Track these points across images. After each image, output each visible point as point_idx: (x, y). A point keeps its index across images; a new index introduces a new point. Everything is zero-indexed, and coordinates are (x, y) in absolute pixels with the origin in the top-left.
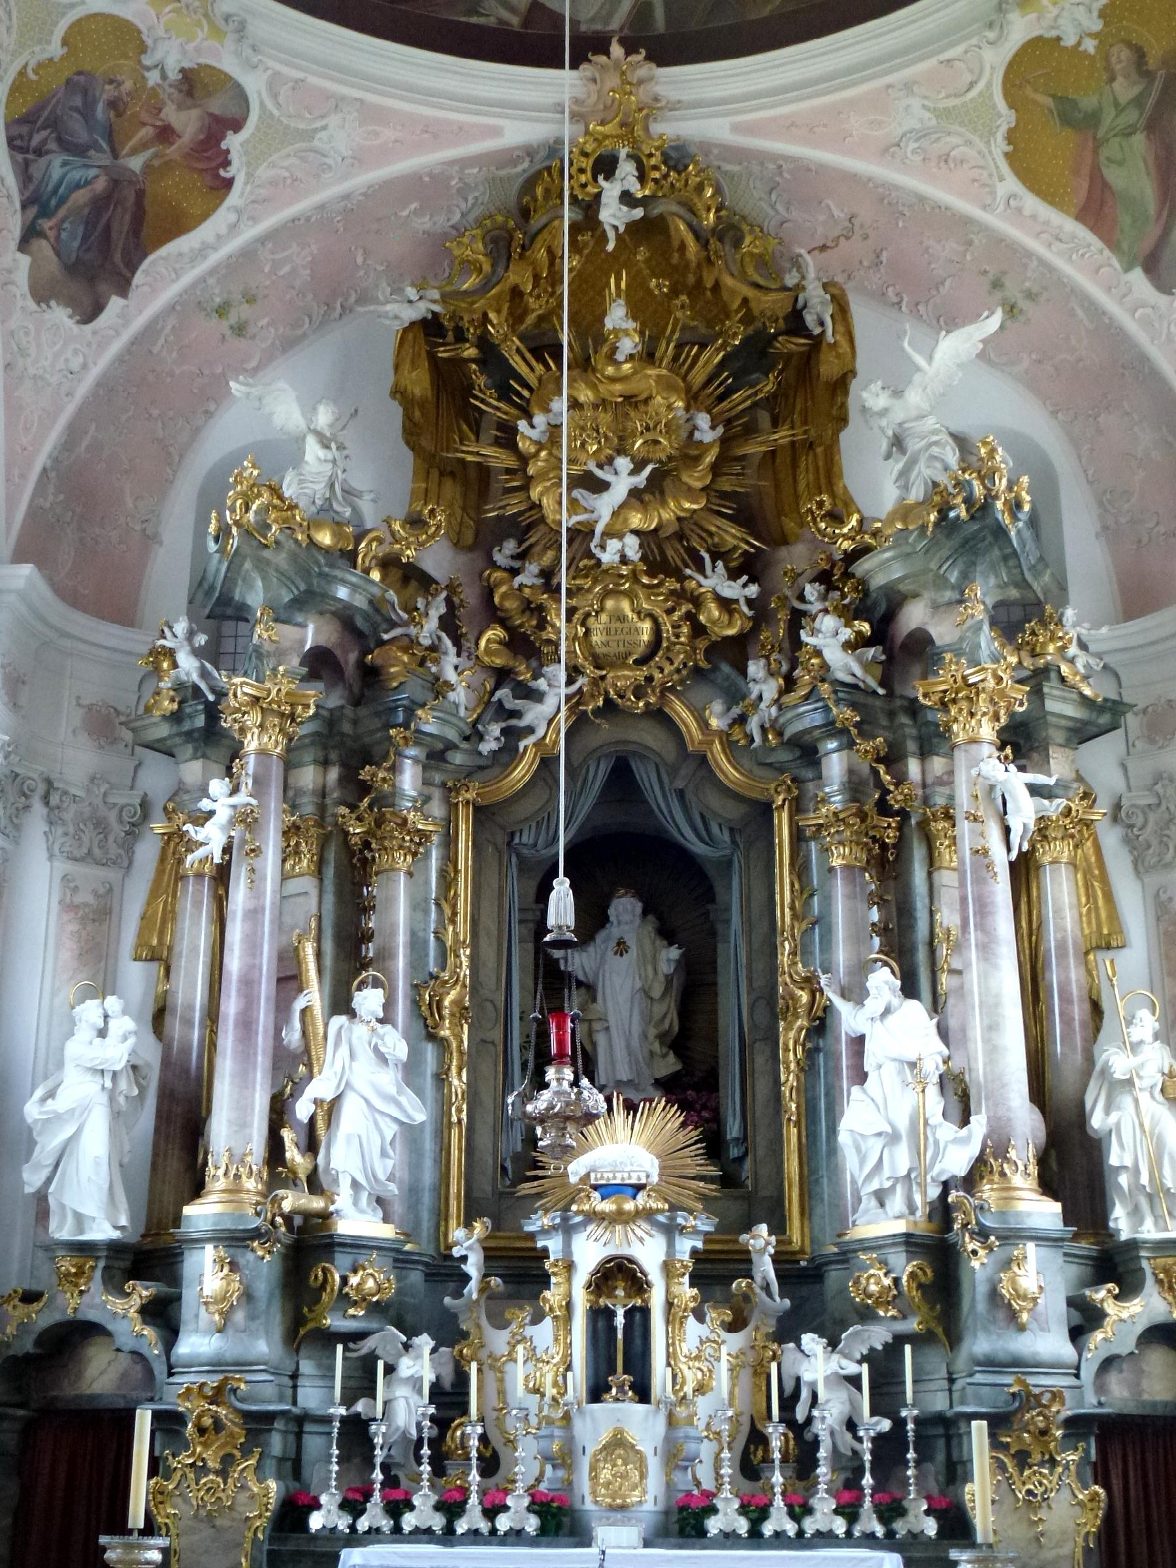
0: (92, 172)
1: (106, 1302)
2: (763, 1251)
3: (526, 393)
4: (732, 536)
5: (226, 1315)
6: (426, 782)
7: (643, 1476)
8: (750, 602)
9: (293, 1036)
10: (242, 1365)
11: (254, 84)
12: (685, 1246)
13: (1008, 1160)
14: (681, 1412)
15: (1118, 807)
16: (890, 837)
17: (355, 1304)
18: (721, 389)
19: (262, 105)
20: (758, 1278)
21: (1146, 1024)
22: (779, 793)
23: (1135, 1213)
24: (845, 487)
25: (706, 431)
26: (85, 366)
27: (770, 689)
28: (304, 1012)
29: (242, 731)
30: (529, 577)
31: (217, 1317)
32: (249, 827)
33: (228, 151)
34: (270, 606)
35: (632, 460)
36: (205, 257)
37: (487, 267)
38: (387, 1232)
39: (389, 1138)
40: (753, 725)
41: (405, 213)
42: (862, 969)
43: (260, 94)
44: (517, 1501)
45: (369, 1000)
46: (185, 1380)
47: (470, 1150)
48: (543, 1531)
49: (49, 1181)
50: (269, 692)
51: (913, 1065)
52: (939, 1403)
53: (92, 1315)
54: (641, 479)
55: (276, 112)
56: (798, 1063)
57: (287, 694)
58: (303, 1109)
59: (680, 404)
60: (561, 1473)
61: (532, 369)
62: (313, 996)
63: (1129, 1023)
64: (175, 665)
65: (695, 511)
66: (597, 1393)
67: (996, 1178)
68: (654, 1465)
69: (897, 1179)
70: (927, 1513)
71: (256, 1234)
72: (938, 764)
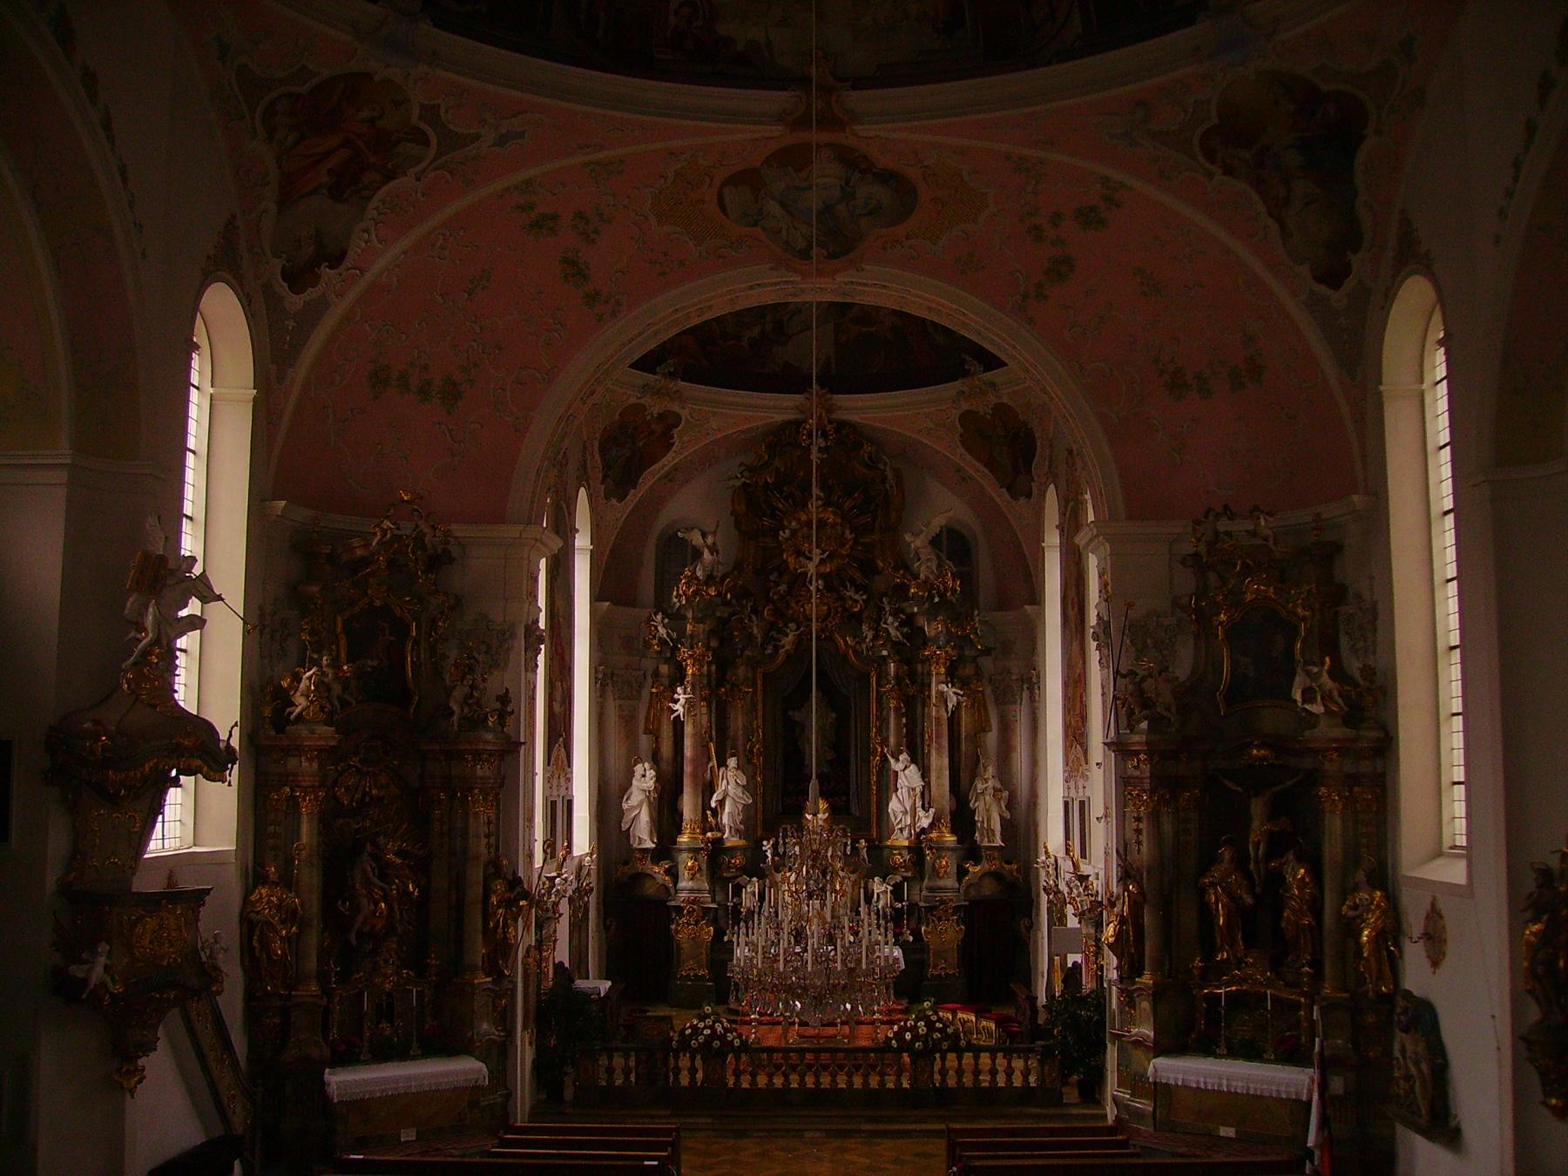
4: (858, 576)
5: (693, 875)
8: (863, 600)
10: (699, 891)
11: (684, 413)
19: (687, 419)
21: (991, 771)
26: (622, 516)
27: (870, 635)
30: (783, 588)
34: (693, 618)
38: (742, 842)
45: (732, 762)
49: (630, 827)
50: (696, 653)
51: (914, 789)
53: (649, 871)
55: (691, 420)
58: (713, 805)
59: (840, 521)
63: (985, 771)
70: (910, 934)
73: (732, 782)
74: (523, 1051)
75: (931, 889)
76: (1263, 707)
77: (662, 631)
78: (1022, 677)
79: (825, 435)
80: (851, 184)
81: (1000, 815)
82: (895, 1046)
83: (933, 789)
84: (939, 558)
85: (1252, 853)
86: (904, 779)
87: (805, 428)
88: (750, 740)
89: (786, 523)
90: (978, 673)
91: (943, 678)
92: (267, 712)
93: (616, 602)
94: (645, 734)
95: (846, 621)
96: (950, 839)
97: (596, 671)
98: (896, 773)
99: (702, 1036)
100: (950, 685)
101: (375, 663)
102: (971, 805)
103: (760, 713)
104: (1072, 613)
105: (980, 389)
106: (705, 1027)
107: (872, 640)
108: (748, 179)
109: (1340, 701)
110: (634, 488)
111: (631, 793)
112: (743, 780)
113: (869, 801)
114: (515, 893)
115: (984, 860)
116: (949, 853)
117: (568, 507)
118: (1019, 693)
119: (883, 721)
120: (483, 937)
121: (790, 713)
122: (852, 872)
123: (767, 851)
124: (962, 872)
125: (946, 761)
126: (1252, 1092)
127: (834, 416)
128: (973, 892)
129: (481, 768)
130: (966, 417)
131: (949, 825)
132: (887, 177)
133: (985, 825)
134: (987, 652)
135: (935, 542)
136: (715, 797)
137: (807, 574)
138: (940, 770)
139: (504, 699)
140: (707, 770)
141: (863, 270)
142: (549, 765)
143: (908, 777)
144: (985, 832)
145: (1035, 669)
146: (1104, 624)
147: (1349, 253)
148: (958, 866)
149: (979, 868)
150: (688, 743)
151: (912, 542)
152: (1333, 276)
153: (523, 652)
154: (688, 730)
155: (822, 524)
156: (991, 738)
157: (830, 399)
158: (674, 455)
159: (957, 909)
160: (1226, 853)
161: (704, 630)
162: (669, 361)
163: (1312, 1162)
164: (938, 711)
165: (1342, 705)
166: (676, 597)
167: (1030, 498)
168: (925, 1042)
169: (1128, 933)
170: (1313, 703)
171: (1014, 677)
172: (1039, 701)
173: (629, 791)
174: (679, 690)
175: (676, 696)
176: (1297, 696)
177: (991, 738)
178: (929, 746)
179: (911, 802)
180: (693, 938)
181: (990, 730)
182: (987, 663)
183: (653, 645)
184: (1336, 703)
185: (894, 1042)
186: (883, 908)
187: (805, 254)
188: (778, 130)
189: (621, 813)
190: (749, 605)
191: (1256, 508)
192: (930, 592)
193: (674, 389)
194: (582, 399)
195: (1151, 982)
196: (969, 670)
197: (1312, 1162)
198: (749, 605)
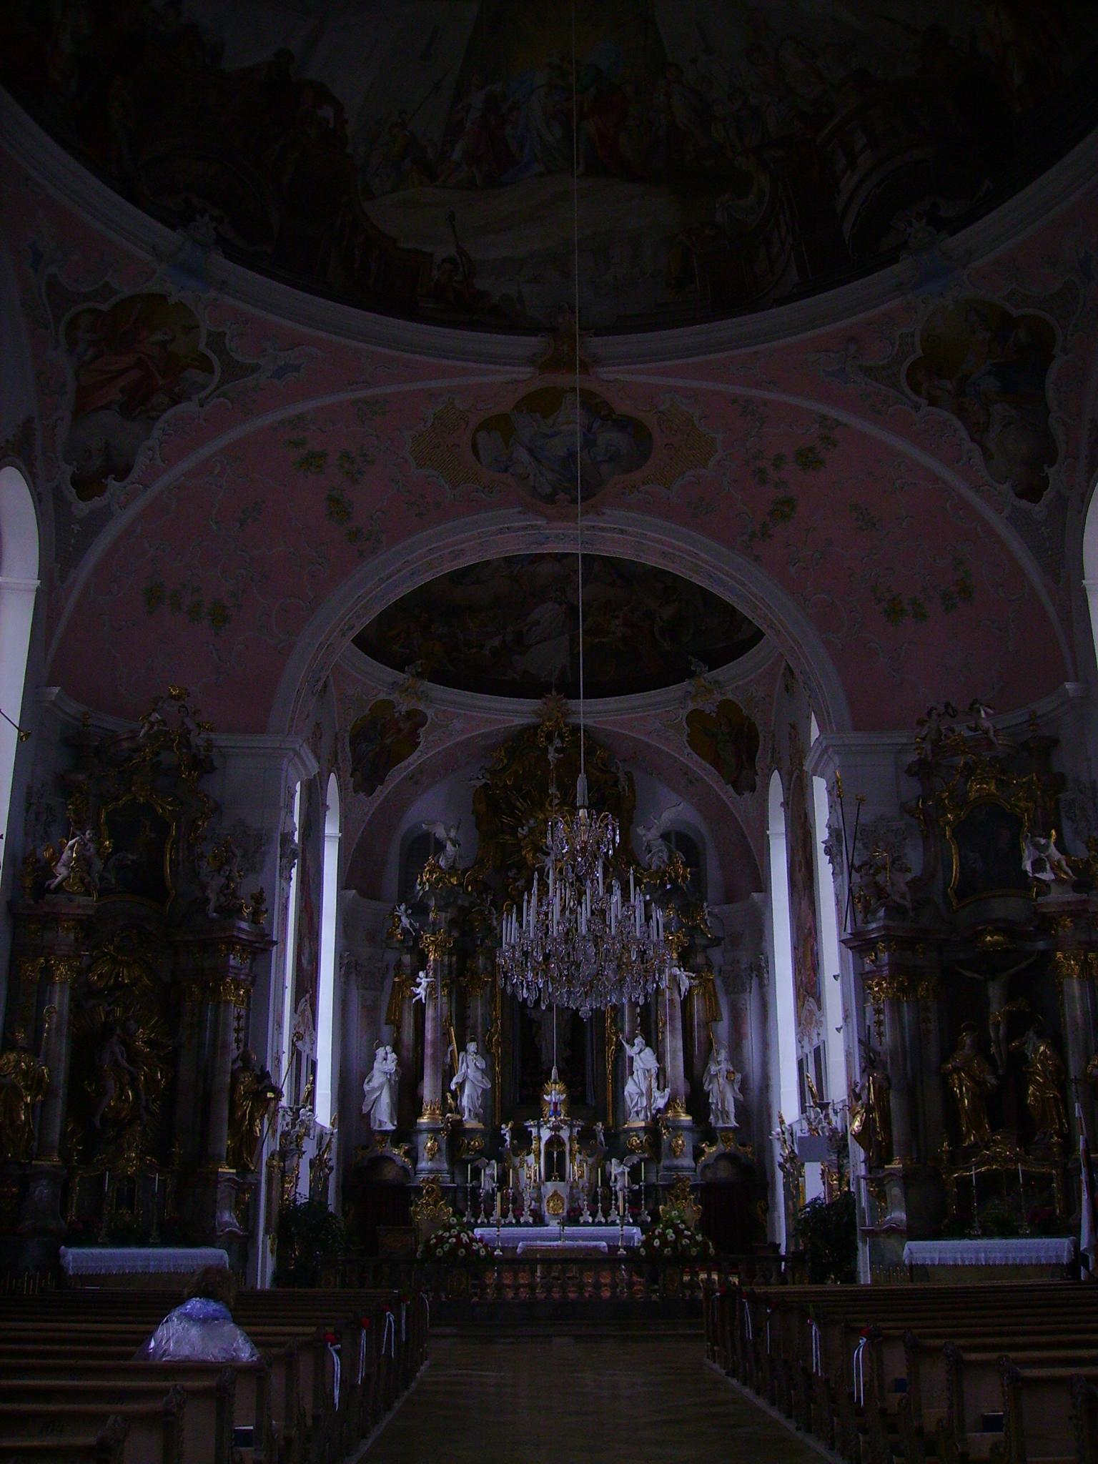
0: (374, 747)
5: (433, 1156)
7: (563, 1204)
10: (439, 1171)
11: (429, 713)
13: (676, 1102)
14: (575, 1185)
15: (721, 969)
17: (472, 1150)
19: (432, 719)
21: (723, 1055)
23: (716, 1117)
26: (368, 812)
28: (451, 1051)
29: (429, 951)
37: (505, 761)
38: (480, 1126)
39: (480, 1092)
43: (431, 715)
44: (526, 1212)
45: (472, 1047)
46: (422, 1176)
48: (534, 1221)
50: (438, 939)
56: (612, 1062)
58: (453, 1087)
60: (538, 1204)
61: (522, 805)
63: (718, 1054)
64: (401, 921)
66: (548, 1179)
67: (673, 1108)
68: (566, 1200)
69: (642, 1108)
71: (442, 1129)
73: (472, 1065)
74: (264, 1257)
75: (668, 1168)
76: (994, 897)
77: (405, 921)
78: (751, 966)
79: (561, 736)
80: (593, 430)
81: (734, 1098)
82: (644, 1254)
83: (669, 1070)
84: (670, 850)
85: (992, 1035)
86: (638, 1059)
87: (542, 731)
88: (490, 1031)
89: (524, 822)
90: (709, 964)
91: (675, 962)
92: (28, 882)
93: (362, 893)
94: (386, 1024)
96: (685, 1118)
98: (631, 1059)
99: (447, 1245)
100: (682, 969)
101: (135, 858)
102: (705, 1088)
103: (499, 1004)
104: (799, 877)
105: (704, 687)
106: (449, 1237)
108: (500, 424)
109: (1070, 872)
111: (372, 1077)
112: (482, 1064)
113: (605, 1089)
114: (263, 1085)
115: (719, 1140)
116: (685, 1133)
120: (229, 1129)
123: (505, 1134)
124: (698, 1153)
125: (680, 1044)
126: (1010, 1262)
128: (709, 1174)
129: (234, 958)
130: (694, 717)
131: (684, 1105)
132: (627, 424)
133: (720, 1107)
134: (716, 941)
135: (665, 836)
136: (455, 1080)
137: (544, 869)
138: (674, 1052)
139: (259, 898)
140: (446, 1054)
141: (603, 514)
142: (296, 1012)
143: (643, 1059)
145: (762, 954)
146: (835, 833)
147: (1045, 467)
148: (693, 1147)
149: (714, 1149)
150: (429, 1026)
151: (644, 835)
152: (1031, 491)
153: (279, 859)
154: (430, 1013)
156: (723, 1028)
158: (420, 753)
159: (694, 1188)
160: (967, 1039)
161: (446, 918)
162: (417, 662)
163: (1087, 1268)
164: (672, 993)
165: (1071, 874)
166: (420, 885)
167: (754, 792)
168: (674, 1248)
169: (874, 1119)
170: (1043, 872)
171: (743, 967)
172: (768, 985)
174: (421, 974)
175: (418, 980)
176: (1028, 866)
177: (723, 1028)
178: (663, 1033)
179: (648, 1082)
180: (431, 1219)
182: (716, 955)
183: (396, 935)
184: (1066, 873)
185: (642, 1249)
187: (550, 499)
188: (525, 372)
189: (363, 1095)
191: (976, 701)
192: (662, 880)
193: (421, 689)
194: (341, 630)
195: (901, 1166)
196: (700, 960)
197: (1087, 1268)
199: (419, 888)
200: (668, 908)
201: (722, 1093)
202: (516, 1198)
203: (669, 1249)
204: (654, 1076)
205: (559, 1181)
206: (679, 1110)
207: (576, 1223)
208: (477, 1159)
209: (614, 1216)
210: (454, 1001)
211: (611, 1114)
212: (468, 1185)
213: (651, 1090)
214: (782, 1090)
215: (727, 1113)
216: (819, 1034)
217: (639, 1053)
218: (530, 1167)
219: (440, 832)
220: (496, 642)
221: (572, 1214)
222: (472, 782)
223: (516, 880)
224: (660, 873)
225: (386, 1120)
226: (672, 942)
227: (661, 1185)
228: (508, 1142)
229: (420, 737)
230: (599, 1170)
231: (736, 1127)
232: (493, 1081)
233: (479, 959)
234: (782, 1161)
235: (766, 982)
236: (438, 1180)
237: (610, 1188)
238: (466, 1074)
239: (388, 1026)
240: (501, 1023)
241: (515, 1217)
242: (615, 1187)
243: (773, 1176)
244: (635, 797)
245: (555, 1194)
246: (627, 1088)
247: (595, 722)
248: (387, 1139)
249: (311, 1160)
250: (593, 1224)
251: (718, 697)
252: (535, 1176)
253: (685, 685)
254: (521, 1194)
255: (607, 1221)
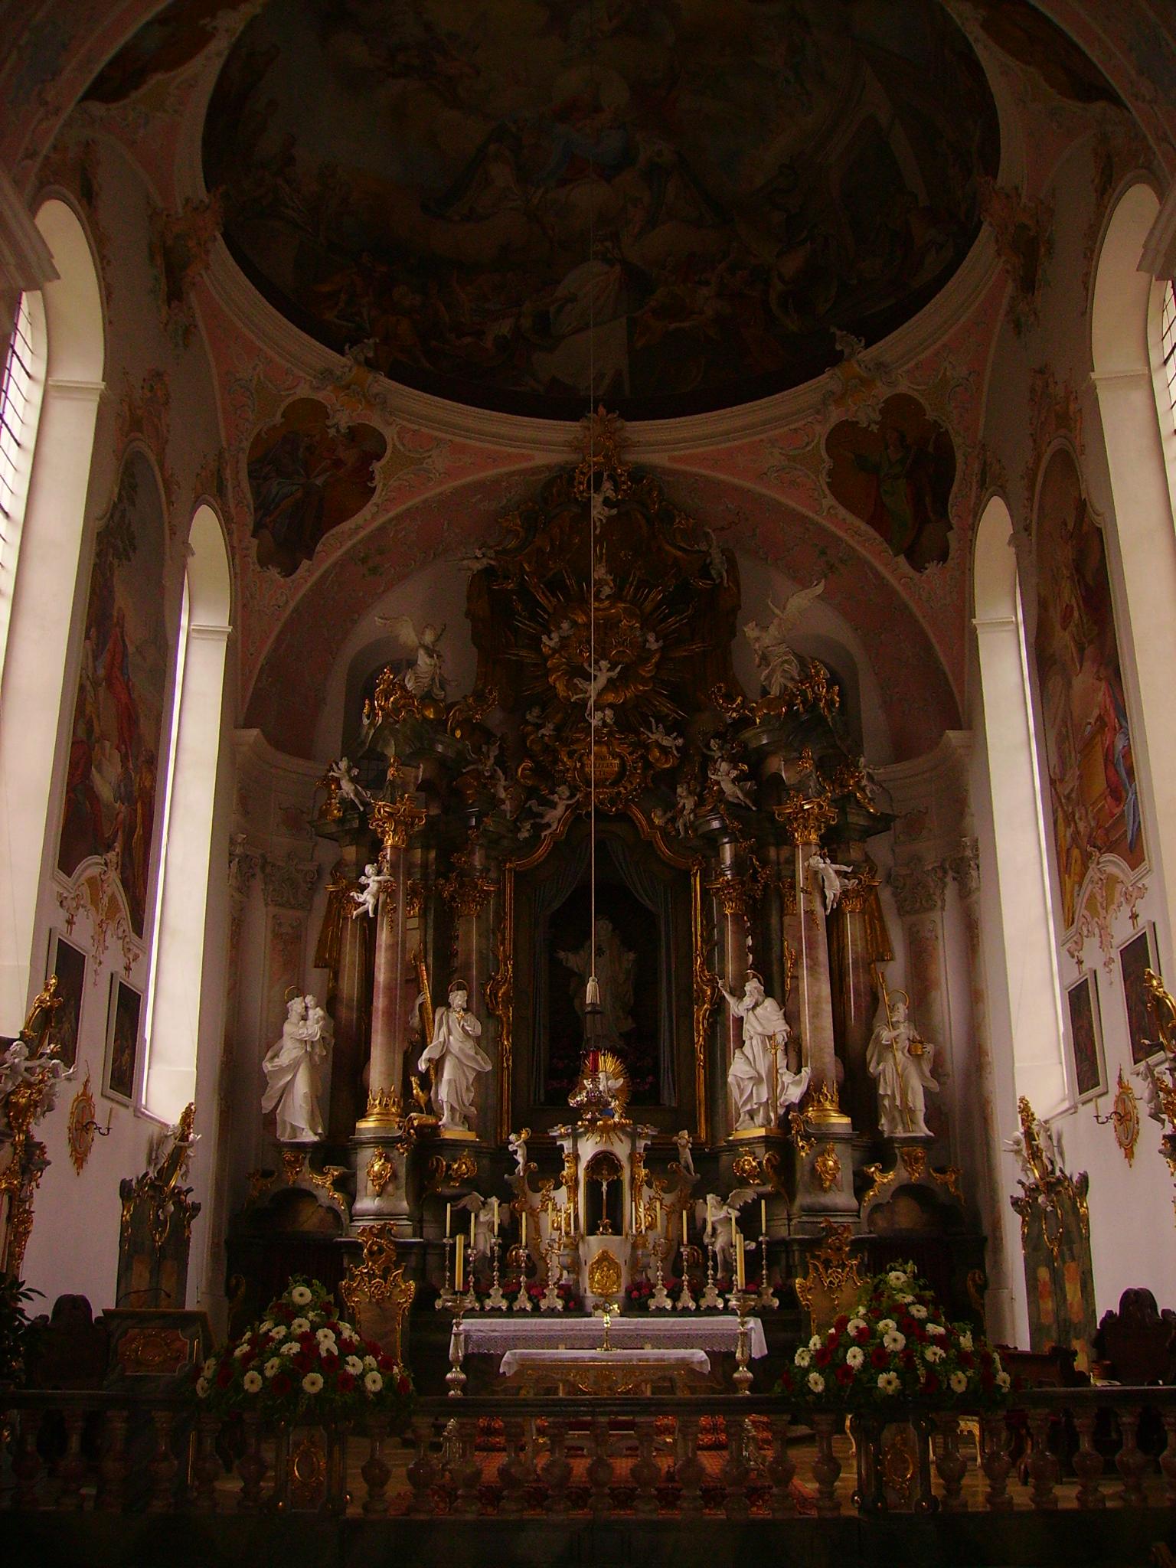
1: (312, 1179)
2: (684, 1147)
3: (546, 616)
4: (666, 707)
5: (383, 1187)
6: (487, 857)
7: (619, 1277)
8: (677, 748)
9: (415, 1021)
10: (394, 1215)
11: (390, 434)
12: (642, 1143)
13: (822, 1093)
14: (640, 1241)
15: (889, 876)
16: (759, 895)
17: (454, 1180)
18: (661, 616)
19: (394, 445)
20: (682, 1162)
21: (901, 1011)
22: (695, 865)
23: (892, 1121)
24: (734, 674)
25: (653, 645)
26: (287, 602)
27: (689, 803)
28: (421, 1005)
29: (384, 833)
30: (547, 731)
31: (377, 1188)
32: (389, 895)
33: (373, 471)
34: (396, 755)
35: (609, 663)
36: (357, 534)
37: (522, 534)
38: (471, 1136)
39: (471, 1078)
40: (680, 824)
41: (474, 500)
42: (743, 979)
44: (552, 1292)
45: (458, 998)
47: (514, 1084)
52: (783, 1232)
54: (614, 674)
55: (402, 449)
56: (705, 1031)
57: (409, 811)
58: (422, 1066)
60: (573, 1276)
61: (550, 602)
62: (427, 996)
64: (340, 788)
65: (646, 691)
66: (592, 1230)
68: (624, 1270)
69: (760, 1104)
70: (773, 1295)
71: (399, 1139)
72: (785, 852)
73: (457, 1031)
75: (811, 1211)
79: (612, 478)
82: (820, 1388)
83: (807, 1037)
87: (582, 473)
88: (491, 978)
91: (814, 849)
93: (276, 741)
95: (651, 785)
96: (839, 1121)
97: (232, 842)
98: (740, 1021)
99: (275, 1361)
100: (828, 861)
103: (508, 934)
104: (1063, 640)
106: (287, 1339)
107: (692, 811)
110: (310, 559)
112: (474, 1027)
116: (838, 1147)
117: (169, 492)
118: (938, 892)
119: (713, 944)
121: (562, 954)
122: (665, 1190)
123: (515, 1152)
124: (862, 1184)
125: (825, 990)
127: (628, 457)
128: (881, 1223)
130: (842, 436)
131: (836, 1098)
133: (898, 1103)
134: (881, 823)
136: (425, 1055)
144: (897, 1114)
148: (855, 1174)
149: (891, 1175)
150: (381, 959)
151: (757, 639)
154: (383, 937)
155: (608, 626)
156: (895, 972)
157: (621, 429)
158: (375, 509)
159: (857, 1245)
172: (978, 889)
173: (276, 1047)
174: (369, 869)
175: (363, 879)
177: (895, 972)
178: (795, 978)
181: (892, 959)
182: (880, 848)
185: (814, 1376)
186: (723, 1250)
189: (263, 1081)
190: (492, 755)
198: (492, 755)
199: (366, 721)
200: (800, 758)
201: (902, 1077)
202: (534, 1265)
203: (892, 1374)
204: (781, 1047)
205: (612, 1234)
206: (828, 1105)
207: (642, 1309)
208: (466, 1195)
209: (712, 1297)
210: (431, 923)
211: (703, 1121)
212: (445, 1241)
213: (777, 1072)
214: (1016, 1065)
215: (912, 1111)
216: (1134, 917)
217: (754, 1008)
218: (560, 1211)
219: (407, 634)
220: (505, 328)
221: (635, 1293)
222: (465, 562)
223: (540, 727)
224: (787, 698)
225: (302, 1125)
226: (809, 815)
227: (800, 1242)
228: (520, 1166)
229: (374, 479)
230: (684, 1213)
231: (928, 1136)
232: (497, 1058)
233: (472, 853)
234: (1020, 1193)
235: (974, 885)
236: (390, 1230)
237: (704, 1248)
238: (445, 1044)
239: (318, 970)
240: (513, 966)
241: (530, 1299)
242: (713, 1244)
243: (997, 1225)
244: (739, 590)
245: (605, 1257)
246: (732, 1071)
247: (672, 459)
248: (304, 1158)
249: (123, 1182)
250: (675, 1312)
251: (883, 391)
252: (569, 1225)
253: (827, 381)
254: (544, 1259)
255: (698, 1307)
